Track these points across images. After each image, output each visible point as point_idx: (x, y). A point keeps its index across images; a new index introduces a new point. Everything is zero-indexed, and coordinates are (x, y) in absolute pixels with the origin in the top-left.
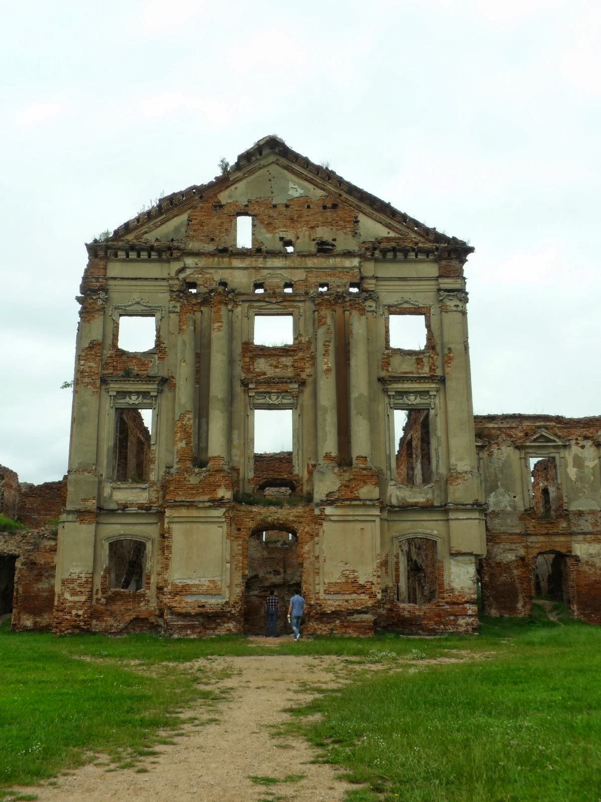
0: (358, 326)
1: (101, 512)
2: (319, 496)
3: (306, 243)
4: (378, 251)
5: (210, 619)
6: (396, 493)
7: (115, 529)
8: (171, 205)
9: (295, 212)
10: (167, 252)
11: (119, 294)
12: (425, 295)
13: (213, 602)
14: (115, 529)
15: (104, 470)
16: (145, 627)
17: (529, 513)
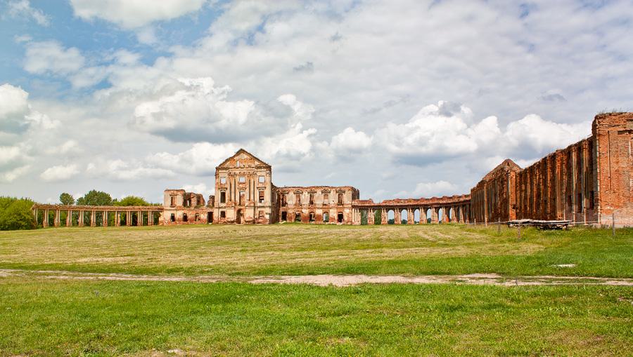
0: (252, 181)
1: (219, 208)
2: (246, 205)
3: (247, 166)
4: (258, 167)
5: (232, 222)
6: (259, 204)
7: (221, 210)
8: (227, 160)
9: (245, 160)
10: (226, 169)
11: (220, 175)
12: (264, 174)
13: (232, 220)
14: (221, 210)
15: (220, 201)
16: (225, 223)
17: (295, 205)
